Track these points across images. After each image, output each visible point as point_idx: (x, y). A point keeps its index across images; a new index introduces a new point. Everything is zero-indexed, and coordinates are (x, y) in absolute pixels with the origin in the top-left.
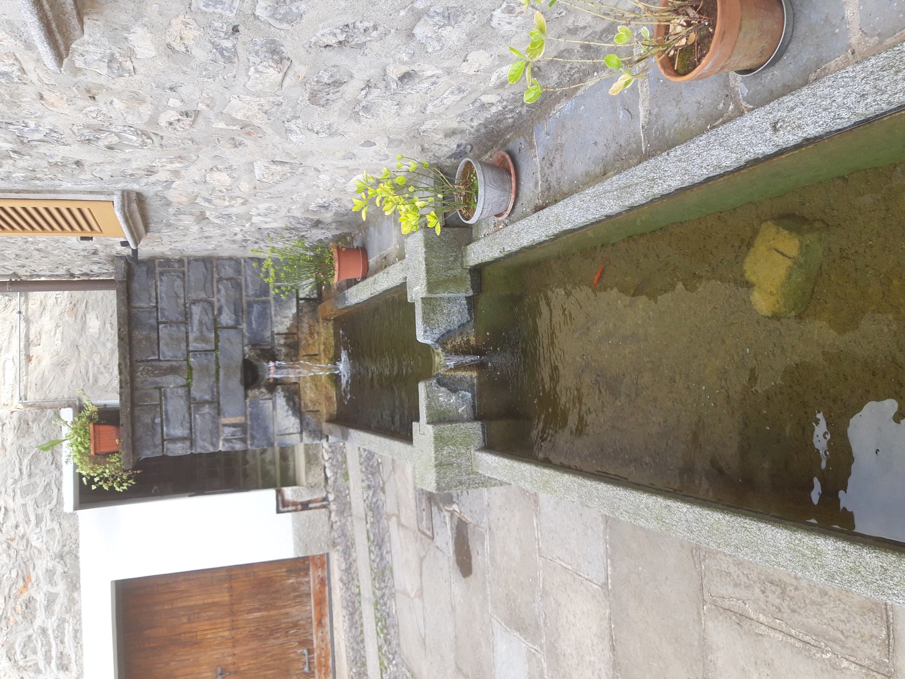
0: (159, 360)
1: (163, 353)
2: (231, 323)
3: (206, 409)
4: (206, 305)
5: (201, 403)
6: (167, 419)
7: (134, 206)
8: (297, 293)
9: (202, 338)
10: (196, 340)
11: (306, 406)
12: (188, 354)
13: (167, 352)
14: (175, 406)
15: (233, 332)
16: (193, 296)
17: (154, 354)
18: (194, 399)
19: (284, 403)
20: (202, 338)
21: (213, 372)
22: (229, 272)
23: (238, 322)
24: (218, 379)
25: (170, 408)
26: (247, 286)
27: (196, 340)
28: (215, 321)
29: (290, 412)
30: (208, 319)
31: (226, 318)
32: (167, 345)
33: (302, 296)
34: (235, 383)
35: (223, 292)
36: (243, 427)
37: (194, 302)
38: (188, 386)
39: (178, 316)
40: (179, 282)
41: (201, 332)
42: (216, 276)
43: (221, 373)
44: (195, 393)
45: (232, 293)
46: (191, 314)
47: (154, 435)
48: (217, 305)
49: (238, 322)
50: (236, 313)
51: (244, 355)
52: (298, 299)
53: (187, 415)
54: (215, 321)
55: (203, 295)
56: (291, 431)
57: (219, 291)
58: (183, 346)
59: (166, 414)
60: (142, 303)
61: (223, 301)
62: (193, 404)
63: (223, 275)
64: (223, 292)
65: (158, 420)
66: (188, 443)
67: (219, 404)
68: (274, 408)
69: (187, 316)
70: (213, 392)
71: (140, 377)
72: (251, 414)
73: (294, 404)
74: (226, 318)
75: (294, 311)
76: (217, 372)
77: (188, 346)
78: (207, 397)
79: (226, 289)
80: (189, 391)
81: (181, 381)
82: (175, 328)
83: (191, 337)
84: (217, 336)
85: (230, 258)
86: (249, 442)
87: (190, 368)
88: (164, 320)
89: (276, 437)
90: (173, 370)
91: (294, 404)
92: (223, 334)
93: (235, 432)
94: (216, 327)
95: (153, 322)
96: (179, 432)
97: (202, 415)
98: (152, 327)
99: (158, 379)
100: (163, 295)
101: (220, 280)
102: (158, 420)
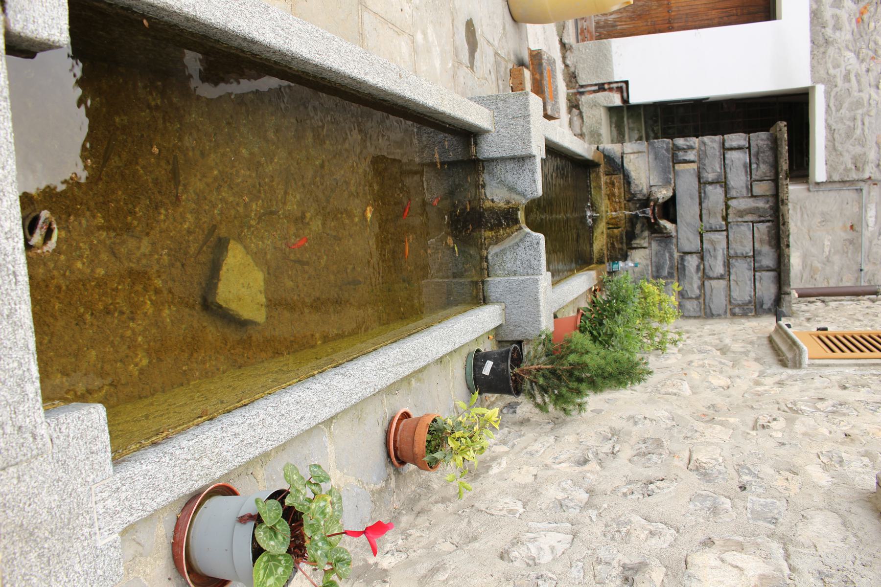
0: (753, 222)
1: (749, 229)
2: (688, 258)
4: (711, 274)
7: (789, 355)
12: (727, 226)
14: (738, 180)
15: (687, 249)
18: (721, 186)
22: (691, 306)
23: (682, 259)
28: (702, 258)
30: (709, 260)
31: (692, 262)
37: (721, 277)
38: (727, 199)
39: (736, 264)
41: (715, 249)
42: (701, 300)
46: (724, 265)
50: (684, 268)
54: (702, 258)
56: (632, 156)
59: (746, 172)
62: (723, 182)
63: (695, 302)
66: (727, 145)
67: (699, 181)
69: (728, 265)
70: (705, 193)
74: (692, 262)
79: (692, 290)
80: (726, 193)
82: (739, 252)
86: (671, 145)
88: (748, 260)
89: (645, 150)
94: (701, 255)
97: (714, 171)
100: (749, 282)
101: (697, 298)
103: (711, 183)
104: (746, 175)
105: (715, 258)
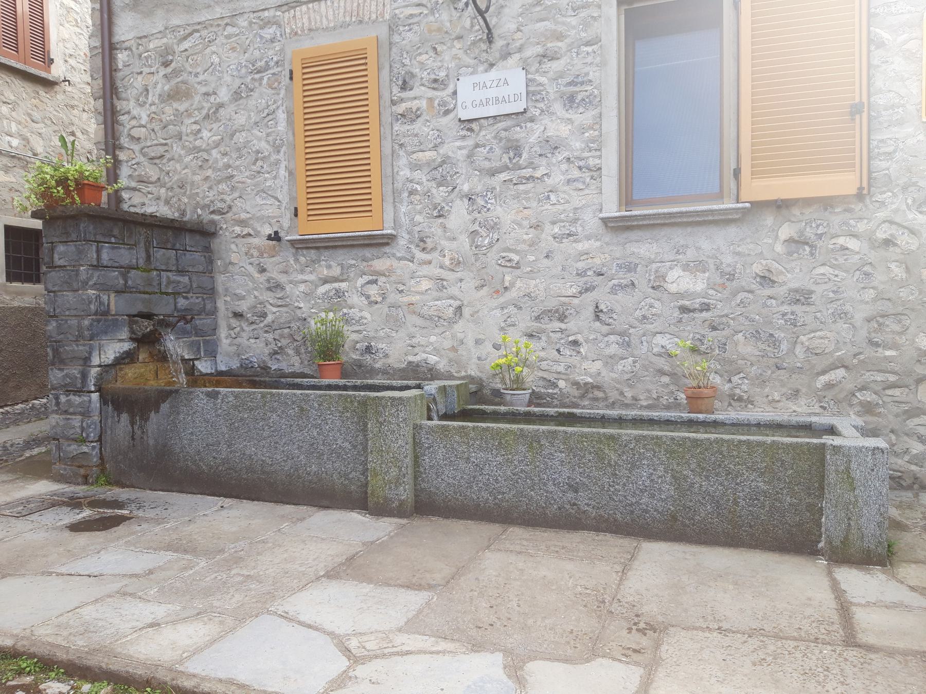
2: (179, 305)
3: (122, 282)
5: (125, 277)
6: (113, 248)
8: (197, 359)
9: (169, 282)
10: (168, 277)
11: (121, 369)
13: (159, 254)
14: (125, 256)
15: (173, 307)
16: (194, 278)
17: (158, 244)
18: (128, 272)
19: (125, 349)
20: (169, 282)
21: (147, 290)
24: (140, 293)
25: (122, 251)
26: (201, 319)
27: (168, 277)
29: (118, 355)
31: (182, 303)
32: (164, 254)
33: (196, 362)
34: (140, 307)
35: (197, 301)
36: (106, 313)
38: (137, 268)
40: (201, 268)
41: (173, 282)
42: (205, 296)
43: (146, 296)
44: (133, 273)
45: (197, 308)
47: (104, 235)
48: (189, 295)
49: (178, 311)
51: (157, 315)
52: (193, 360)
53: (117, 265)
54: (179, 293)
55: (194, 286)
57: (197, 298)
58: (163, 267)
60: (188, 240)
61: (192, 300)
62: (126, 270)
63: (207, 302)
64: (197, 301)
65: (113, 240)
66: (95, 263)
68: (121, 340)
69: (181, 272)
71: (143, 230)
72: (117, 320)
73: (123, 359)
75: (187, 357)
76: (147, 293)
77: (163, 270)
78: (130, 282)
81: (141, 262)
83: (169, 274)
84: (167, 294)
85: (216, 308)
87: (150, 271)
89: (97, 342)
90: (148, 257)
91: (123, 359)
92: (171, 299)
93: (104, 304)
94: (176, 294)
95: (178, 246)
96: (105, 256)
97: (117, 278)
98: (174, 245)
99: (142, 244)
101: (203, 300)
102: (113, 240)
103: (126, 282)
104: (120, 248)
105: (179, 282)
